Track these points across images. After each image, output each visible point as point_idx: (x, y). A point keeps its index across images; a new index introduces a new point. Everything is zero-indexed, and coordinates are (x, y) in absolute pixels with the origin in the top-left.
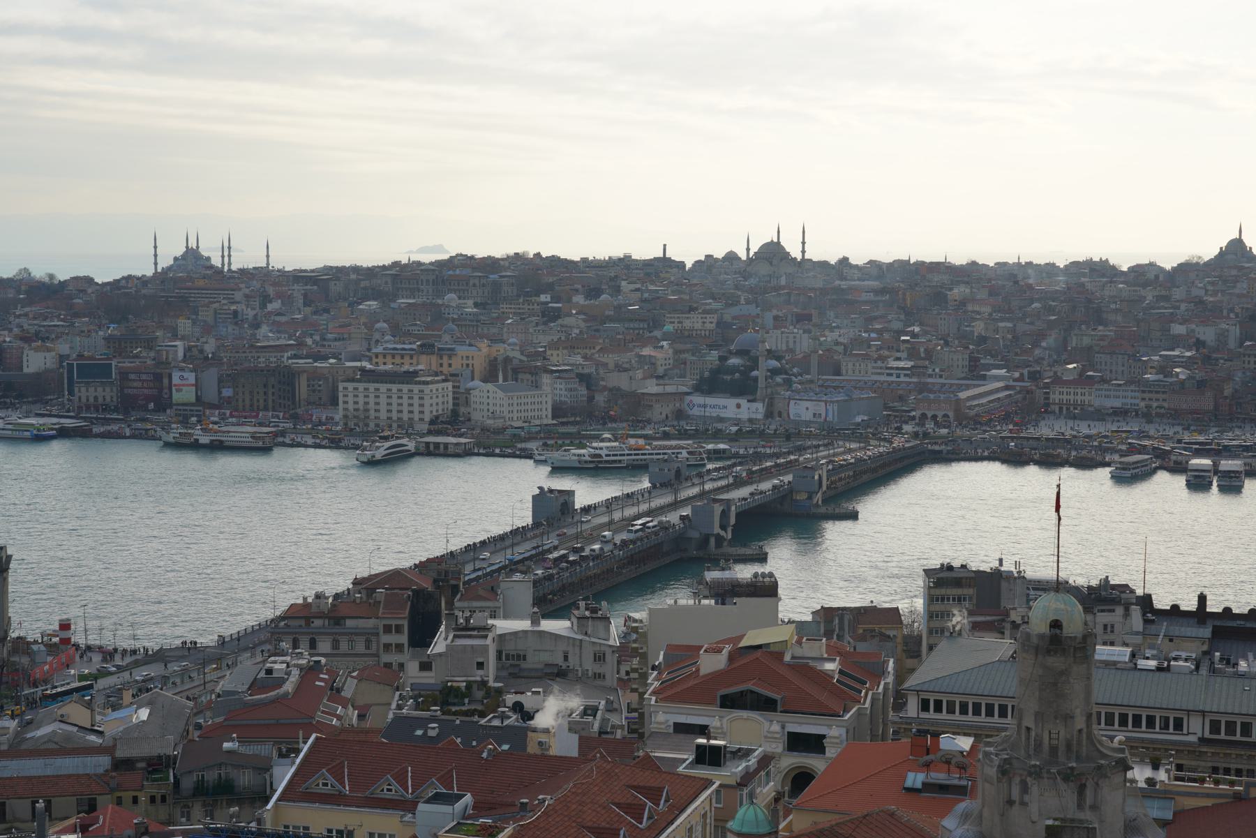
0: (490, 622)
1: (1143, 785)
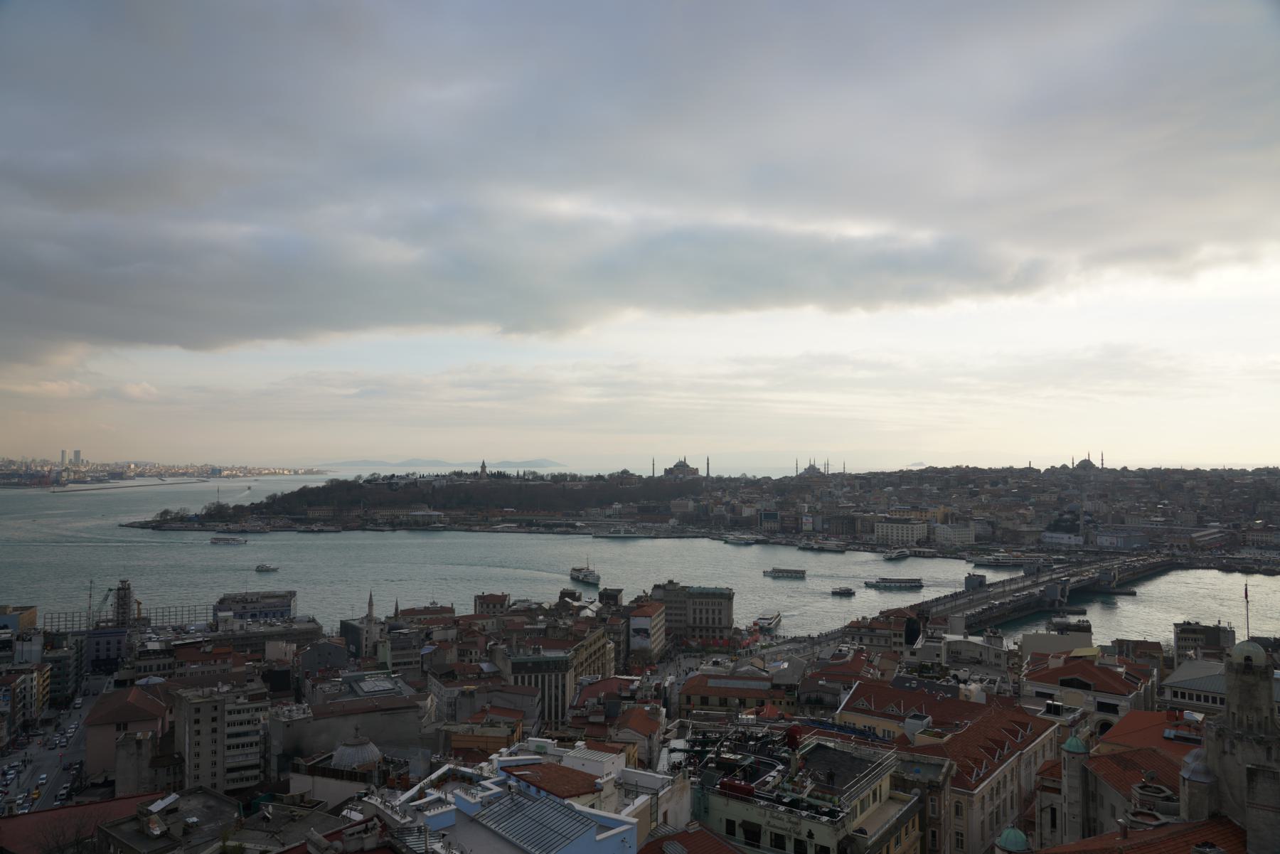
0: (943, 635)
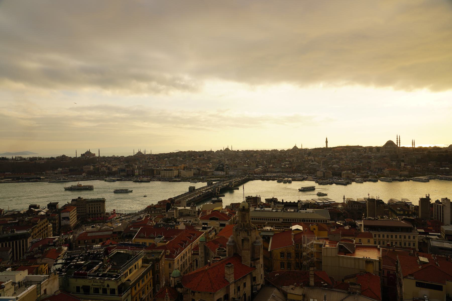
0: (177, 208)
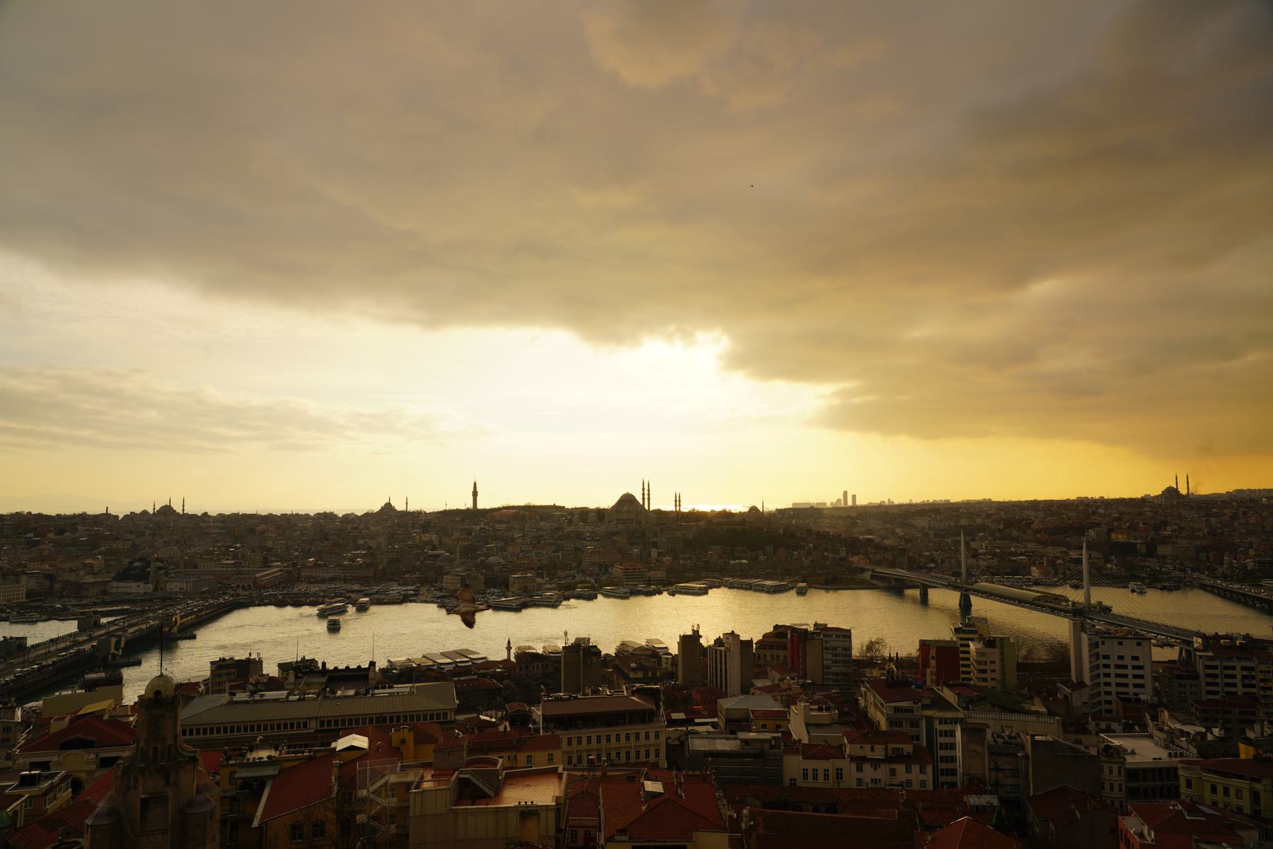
1: (267, 760)
